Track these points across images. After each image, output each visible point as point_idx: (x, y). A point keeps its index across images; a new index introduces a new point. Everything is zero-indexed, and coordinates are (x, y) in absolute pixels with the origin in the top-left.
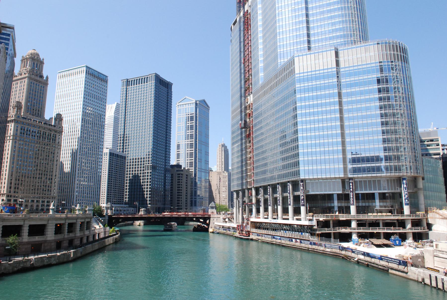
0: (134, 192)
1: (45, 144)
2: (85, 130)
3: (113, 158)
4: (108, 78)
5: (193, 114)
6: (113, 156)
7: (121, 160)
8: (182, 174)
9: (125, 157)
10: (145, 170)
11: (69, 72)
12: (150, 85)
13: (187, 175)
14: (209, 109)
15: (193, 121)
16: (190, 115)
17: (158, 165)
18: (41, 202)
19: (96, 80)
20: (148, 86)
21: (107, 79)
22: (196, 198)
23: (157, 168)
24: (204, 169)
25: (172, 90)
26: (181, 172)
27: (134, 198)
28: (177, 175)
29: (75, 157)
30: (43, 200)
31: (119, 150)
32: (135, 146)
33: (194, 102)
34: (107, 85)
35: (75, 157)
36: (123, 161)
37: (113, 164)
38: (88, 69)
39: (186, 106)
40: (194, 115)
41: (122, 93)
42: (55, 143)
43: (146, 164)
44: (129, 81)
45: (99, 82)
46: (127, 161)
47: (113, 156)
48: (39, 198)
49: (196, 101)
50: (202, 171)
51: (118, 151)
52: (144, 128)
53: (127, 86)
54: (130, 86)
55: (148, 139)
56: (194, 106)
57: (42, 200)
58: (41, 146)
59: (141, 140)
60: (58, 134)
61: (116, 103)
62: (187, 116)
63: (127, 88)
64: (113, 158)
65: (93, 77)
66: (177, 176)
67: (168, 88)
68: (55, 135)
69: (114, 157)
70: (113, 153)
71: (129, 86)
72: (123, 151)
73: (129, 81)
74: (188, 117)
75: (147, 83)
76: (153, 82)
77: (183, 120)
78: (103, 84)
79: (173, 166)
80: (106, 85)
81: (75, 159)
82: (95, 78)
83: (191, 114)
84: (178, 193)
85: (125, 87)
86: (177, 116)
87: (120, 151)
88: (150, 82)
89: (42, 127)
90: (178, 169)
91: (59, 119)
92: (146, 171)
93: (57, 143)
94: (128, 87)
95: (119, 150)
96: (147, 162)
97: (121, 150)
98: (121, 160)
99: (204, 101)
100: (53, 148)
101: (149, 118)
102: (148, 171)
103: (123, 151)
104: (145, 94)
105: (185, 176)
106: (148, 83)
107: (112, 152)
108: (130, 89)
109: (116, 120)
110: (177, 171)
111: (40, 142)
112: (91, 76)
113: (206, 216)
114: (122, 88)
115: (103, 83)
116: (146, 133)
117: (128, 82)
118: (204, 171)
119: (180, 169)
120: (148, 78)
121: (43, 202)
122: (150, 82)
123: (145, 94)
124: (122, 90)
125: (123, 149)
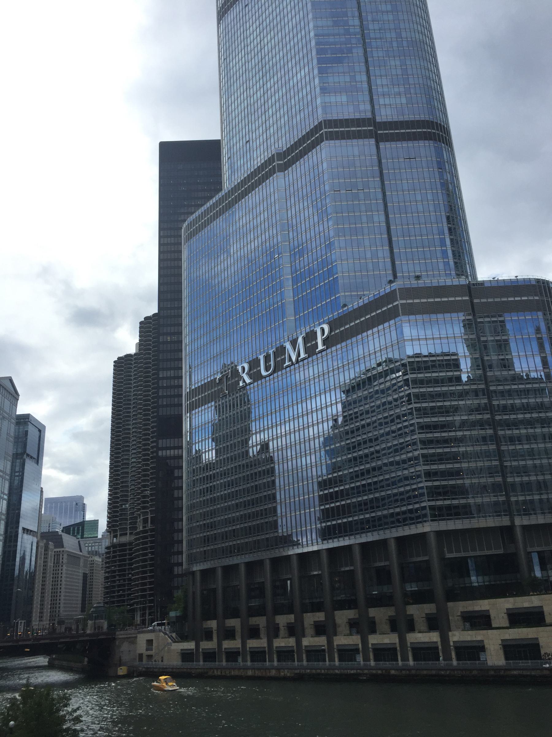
113: (100, 637)
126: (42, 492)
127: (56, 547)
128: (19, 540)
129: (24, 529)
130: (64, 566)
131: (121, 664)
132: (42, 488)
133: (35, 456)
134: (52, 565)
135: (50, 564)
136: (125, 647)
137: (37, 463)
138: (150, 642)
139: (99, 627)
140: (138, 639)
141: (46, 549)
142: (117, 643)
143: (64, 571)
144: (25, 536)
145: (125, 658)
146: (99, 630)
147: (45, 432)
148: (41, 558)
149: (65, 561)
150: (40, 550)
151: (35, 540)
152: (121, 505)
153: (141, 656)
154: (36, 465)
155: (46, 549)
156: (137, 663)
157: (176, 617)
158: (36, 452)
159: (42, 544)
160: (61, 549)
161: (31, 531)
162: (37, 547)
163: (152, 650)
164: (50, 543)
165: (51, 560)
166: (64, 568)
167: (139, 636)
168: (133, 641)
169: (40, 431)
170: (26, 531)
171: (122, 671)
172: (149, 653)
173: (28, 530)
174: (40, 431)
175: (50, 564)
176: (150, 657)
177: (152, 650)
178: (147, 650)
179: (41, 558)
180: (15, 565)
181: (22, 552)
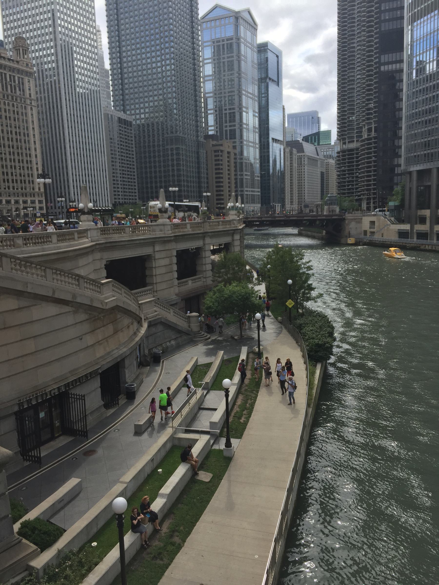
0: (151, 182)
5: (232, 39)
8: (222, 151)
10: (167, 145)
13: (229, 153)
14: (257, 30)
16: (225, 42)
18: (21, 202)
22: (242, 191)
26: (221, 148)
27: (152, 192)
28: (213, 152)
29: (61, 121)
30: (25, 199)
35: (61, 121)
36: (128, 129)
40: (234, 41)
42: (24, 95)
43: (168, 133)
48: (26, 196)
57: (15, 199)
62: (221, 43)
66: (214, 154)
68: (22, 79)
74: (223, 45)
79: (207, 137)
83: (228, 40)
84: (217, 182)
90: (215, 142)
91: (22, 47)
92: (169, 147)
93: (28, 96)
98: (125, 128)
102: (172, 147)
105: (226, 155)
110: (213, 145)
113: (334, 217)
121: (25, 202)
126: (284, 109)
127: (298, 152)
128: (271, 147)
129: (273, 139)
130: (306, 166)
131: (350, 236)
132: (283, 106)
133: (276, 80)
134: (297, 165)
135: (295, 165)
136: (353, 225)
137: (278, 85)
138: (372, 223)
139: (333, 211)
140: (363, 220)
141: (291, 153)
142: (347, 222)
143: (306, 170)
144: (275, 144)
145: (353, 232)
146: (333, 212)
147: (281, 57)
148: (287, 161)
149: (306, 162)
150: (286, 154)
151: (282, 147)
152: (349, 117)
153: (365, 232)
154: (277, 87)
155: (291, 153)
156: (362, 236)
157: (395, 206)
158: (276, 76)
159: (288, 150)
160: (303, 154)
161: (279, 140)
162: (284, 153)
163: (374, 228)
164: (294, 149)
165: (295, 162)
166: (306, 167)
167: (363, 218)
168: (359, 221)
169: (277, 56)
170: (275, 140)
171: (351, 241)
172: (372, 230)
173: (276, 140)
174: (277, 56)
175: (295, 165)
176: (373, 233)
177: (374, 228)
178: (370, 228)
179: (287, 161)
180: (269, 166)
181: (274, 157)
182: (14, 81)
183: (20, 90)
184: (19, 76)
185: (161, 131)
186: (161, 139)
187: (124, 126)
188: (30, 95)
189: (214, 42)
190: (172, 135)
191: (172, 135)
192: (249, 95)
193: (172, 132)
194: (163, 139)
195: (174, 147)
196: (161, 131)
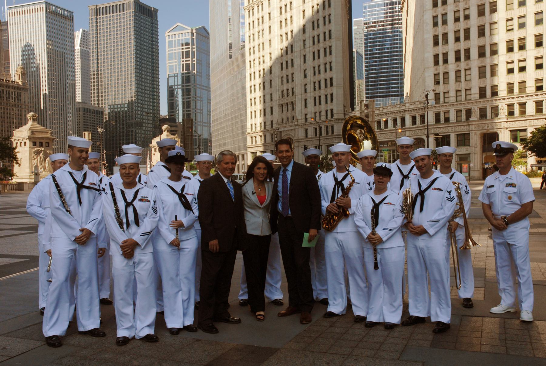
1: (10, 105)
2: (53, 85)
3: (88, 114)
4: (74, 14)
6: (87, 112)
7: (97, 116)
9: (102, 112)
11: (23, 8)
12: (128, 15)
15: (189, 58)
17: (144, 121)
19: (59, 19)
20: (125, 16)
21: (72, 15)
23: (144, 125)
24: (207, 122)
25: (158, 20)
29: (45, 117)
31: (93, 103)
32: (113, 97)
33: (190, 31)
34: (74, 24)
35: (45, 117)
37: (87, 120)
38: (48, 6)
39: (179, 37)
41: (91, 25)
42: (20, 103)
43: (129, 120)
44: (100, 8)
45: (63, 21)
46: (105, 117)
47: (87, 112)
49: (192, 30)
50: (203, 126)
51: (93, 103)
52: (123, 73)
53: (97, 16)
54: (101, 16)
55: (130, 87)
56: (190, 37)
58: (6, 108)
59: (120, 89)
60: (23, 92)
61: (81, 30)
63: (97, 18)
64: (88, 114)
65: (55, 15)
67: (152, 17)
68: (20, 93)
69: (89, 113)
70: (87, 109)
71: (100, 15)
72: (98, 104)
73: (100, 8)
75: (123, 11)
76: (132, 11)
77: (175, 57)
78: (68, 23)
80: (72, 24)
81: (45, 120)
82: (58, 16)
85: (94, 17)
86: (167, 50)
87: (94, 104)
88: (128, 11)
89: (4, 85)
93: (23, 103)
94: (98, 17)
95: (93, 103)
96: (130, 118)
97: (96, 102)
98: (97, 116)
99: (204, 28)
100: (20, 109)
101: (129, 61)
103: (98, 104)
104: (122, 28)
106: (125, 12)
107: (86, 107)
108: (102, 20)
109: (85, 55)
111: (4, 103)
112: (53, 15)
114: (91, 18)
115: (68, 22)
116: (127, 80)
117: (98, 11)
118: (206, 125)
119: (175, 125)
120: (125, 5)
122: (128, 11)
123: (122, 28)
124: (91, 21)
125: (98, 100)
182: (15, 95)
183: (18, 100)
184: (18, 91)
185: (125, 118)
186: (125, 124)
187: (96, 115)
188: (25, 102)
189: (182, 45)
190: (132, 121)
191: (132, 121)
192: (203, 88)
193: (132, 119)
194: (126, 123)
195: (134, 129)
196: (125, 118)
